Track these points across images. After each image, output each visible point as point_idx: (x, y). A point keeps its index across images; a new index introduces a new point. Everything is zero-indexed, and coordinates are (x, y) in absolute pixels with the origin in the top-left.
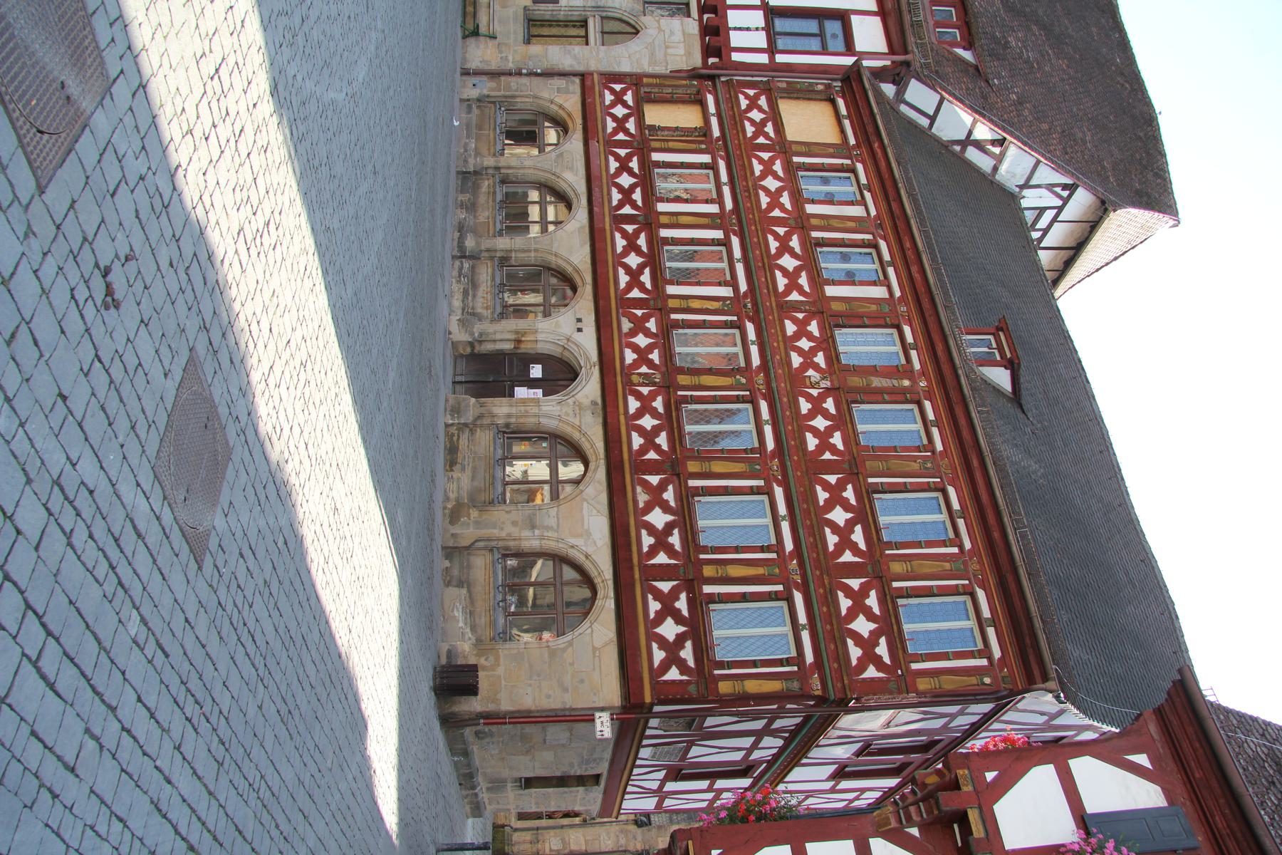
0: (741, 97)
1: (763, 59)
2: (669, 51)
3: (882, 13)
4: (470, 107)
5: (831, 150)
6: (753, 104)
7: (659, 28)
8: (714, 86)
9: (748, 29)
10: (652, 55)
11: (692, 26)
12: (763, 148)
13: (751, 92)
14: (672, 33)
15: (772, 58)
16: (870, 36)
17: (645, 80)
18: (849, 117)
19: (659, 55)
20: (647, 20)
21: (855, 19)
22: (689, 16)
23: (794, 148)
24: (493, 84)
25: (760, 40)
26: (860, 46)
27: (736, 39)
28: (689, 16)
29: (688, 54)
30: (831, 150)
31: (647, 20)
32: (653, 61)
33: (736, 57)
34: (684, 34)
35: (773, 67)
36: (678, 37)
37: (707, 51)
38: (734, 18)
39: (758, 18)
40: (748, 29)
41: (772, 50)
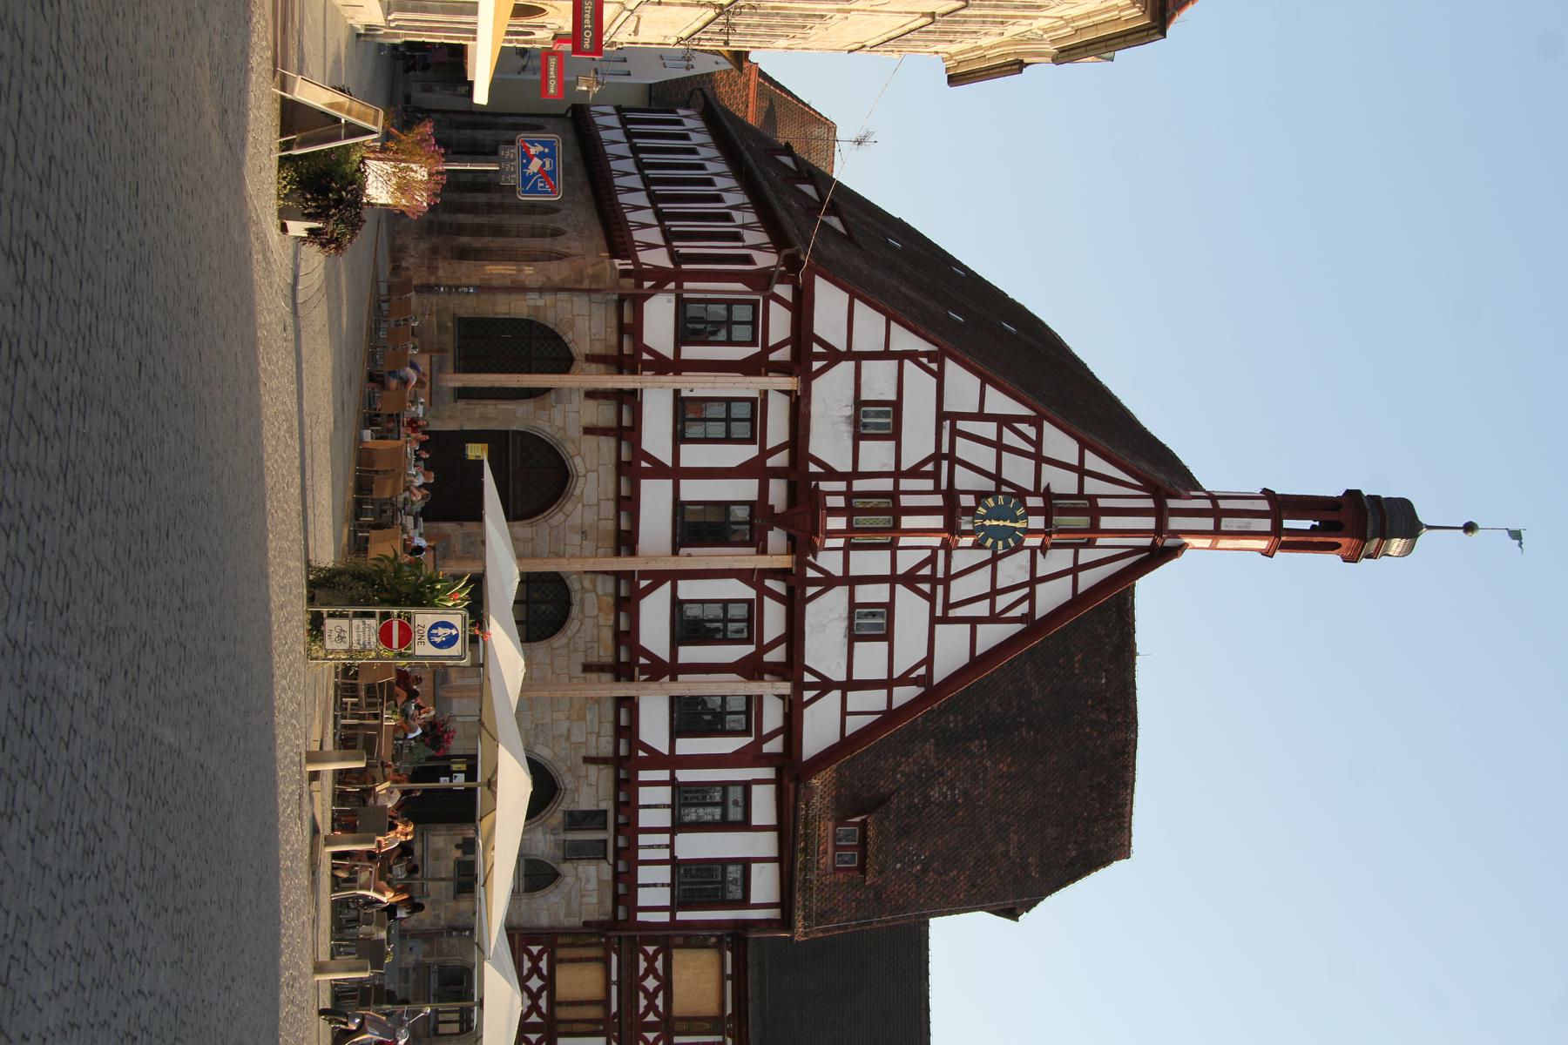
0: (641, 957)
1: (664, 917)
2: (585, 900)
3: (778, 860)
4: (407, 975)
5: (708, 1026)
6: (651, 970)
7: (577, 877)
8: (620, 943)
9: (655, 885)
10: (569, 904)
11: (606, 870)
12: (651, 1027)
13: (650, 949)
14: (588, 881)
15: (673, 916)
16: (765, 883)
17: (560, 940)
18: (731, 977)
19: (575, 905)
20: (566, 868)
21: (755, 867)
22: (605, 858)
23: (678, 1026)
24: (426, 947)
25: (663, 897)
26: (753, 901)
27: (645, 897)
28: (605, 858)
29: (601, 903)
30: (708, 1026)
31: (566, 868)
32: (568, 914)
33: (641, 917)
34: (599, 880)
35: (673, 924)
36: (593, 884)
37: (617, 899)
38: (644, 874)
39: (664, 874)
40: (655, 885)
41: (672, 909)
